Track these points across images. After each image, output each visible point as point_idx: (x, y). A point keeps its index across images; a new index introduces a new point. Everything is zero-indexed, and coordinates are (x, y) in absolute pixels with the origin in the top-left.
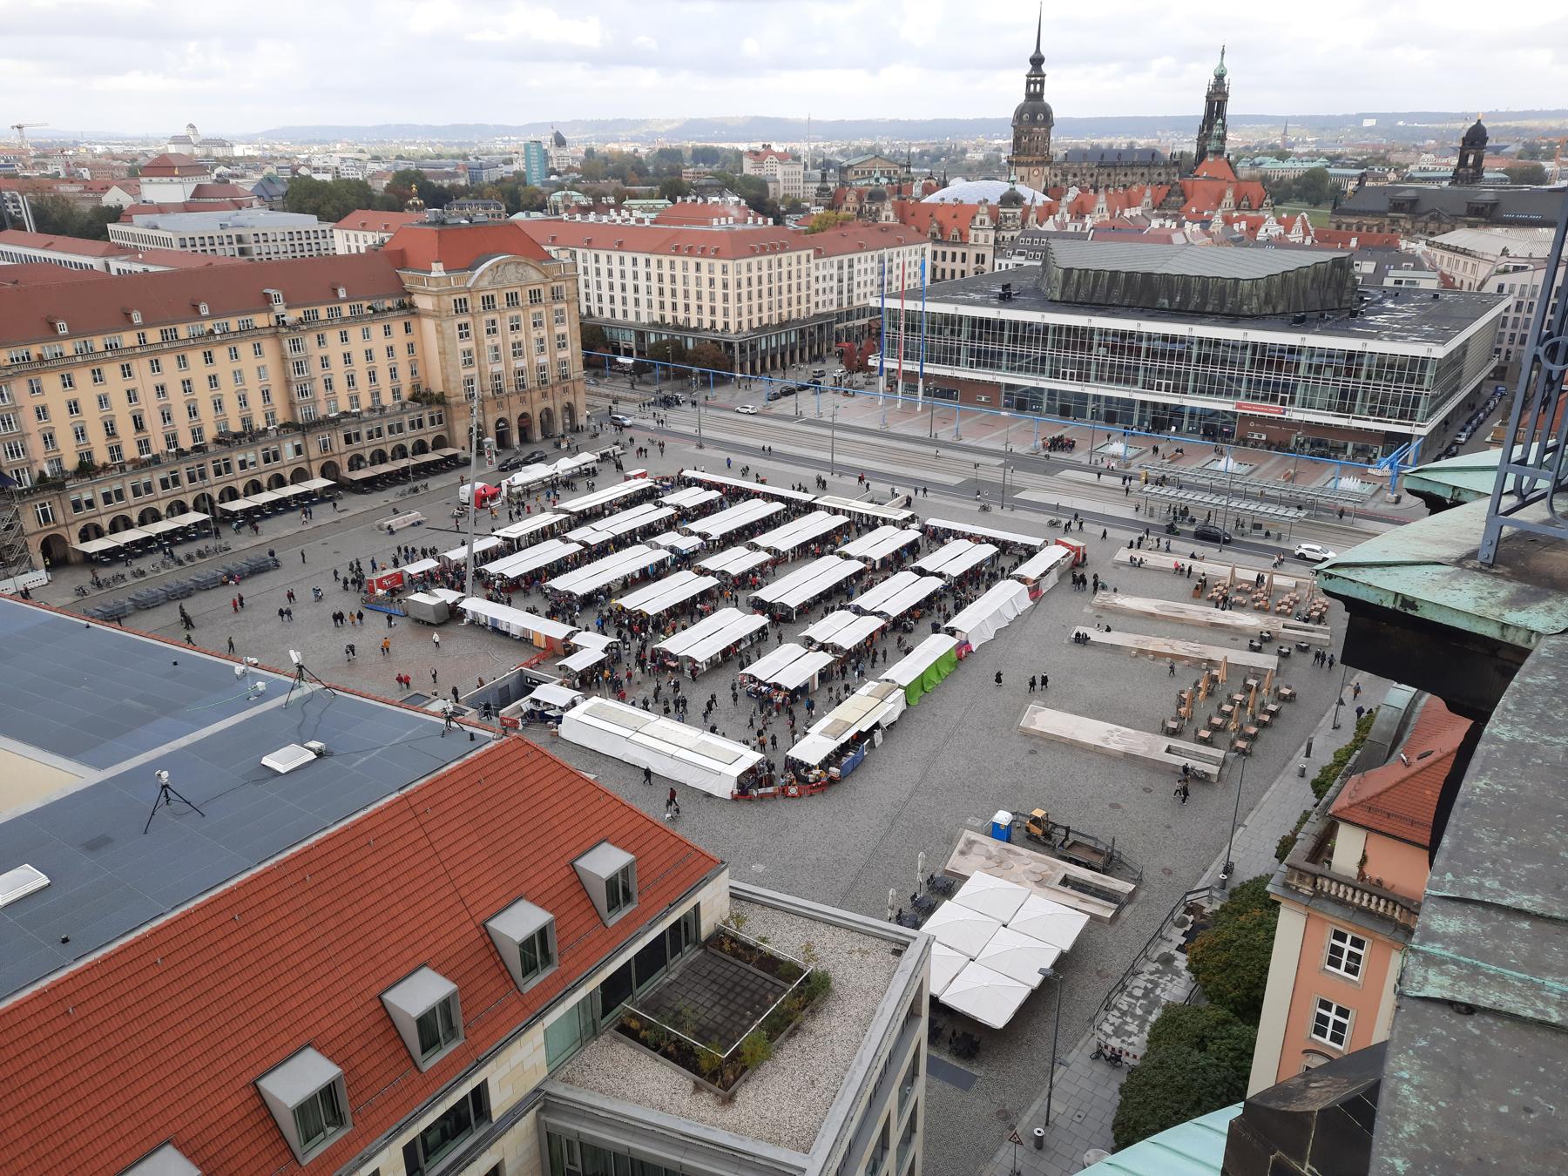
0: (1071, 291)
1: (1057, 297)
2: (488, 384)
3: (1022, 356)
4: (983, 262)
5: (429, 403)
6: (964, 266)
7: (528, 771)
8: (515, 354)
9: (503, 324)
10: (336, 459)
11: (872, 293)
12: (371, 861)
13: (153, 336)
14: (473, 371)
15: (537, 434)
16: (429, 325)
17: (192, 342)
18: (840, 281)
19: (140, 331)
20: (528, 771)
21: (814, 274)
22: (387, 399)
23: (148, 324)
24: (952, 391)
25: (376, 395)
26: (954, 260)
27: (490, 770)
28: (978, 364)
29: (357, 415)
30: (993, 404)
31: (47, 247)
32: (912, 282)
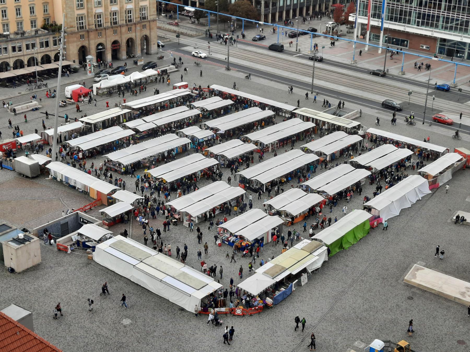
2: (92, 20)
3: (453, 19)
5: (54, 31)
14: (84, 12)
15: (123, 55)
22: (27, 28)
24: (403, 41)
25: (20, 23)
28: (423, 24)
29: (6, 36)
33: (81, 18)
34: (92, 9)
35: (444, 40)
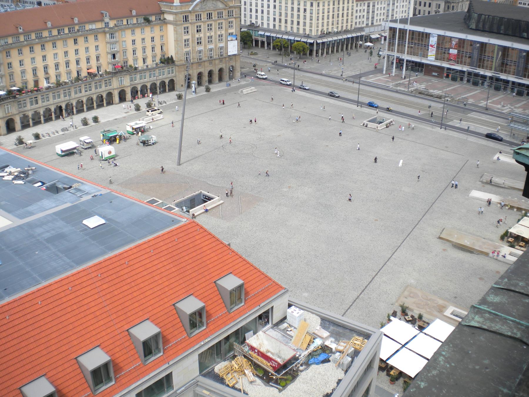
0: (481, 26)
1: (474, 27)
4: (439, 8)
6: (429, 9)
7: (197, 237)
8: (209, 42)
9: (204, 27)
11: (383, 19)
12: (126, 271)
16: (170, 28)
18: (368, 12)
20: (197, 237)
21: (355, 8)
23: (53, 27)
26: (425, 6)
27: (181, 235)
30: (440, 76)
32: (404, 15)
33: (187, 53)
34: (195, 47)
35: (449, 69)
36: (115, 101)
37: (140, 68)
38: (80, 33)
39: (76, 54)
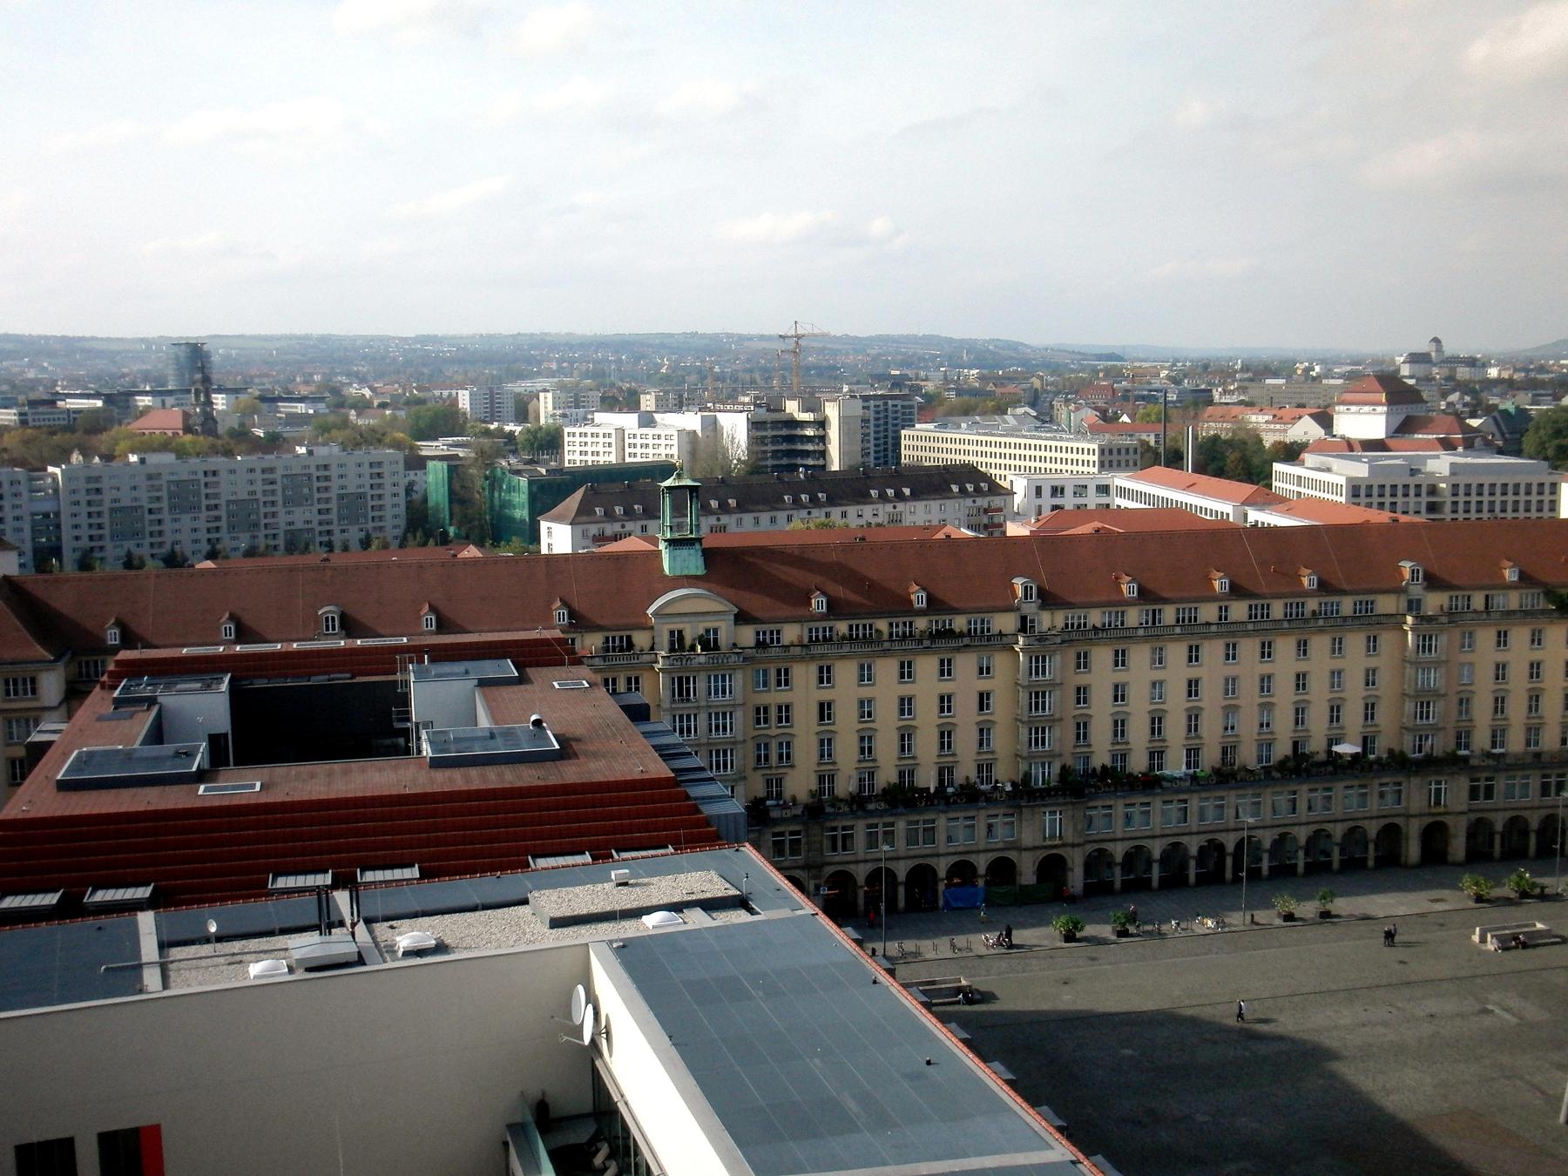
10: (1448, 820)
13: (1239, 610)
17: (1286, 625)
19: (1223, 604)
31: (1190, 487)
36: (1407, 857)
37: (1508, 761)
38: (1321, 622)
39: (1190, 695)
